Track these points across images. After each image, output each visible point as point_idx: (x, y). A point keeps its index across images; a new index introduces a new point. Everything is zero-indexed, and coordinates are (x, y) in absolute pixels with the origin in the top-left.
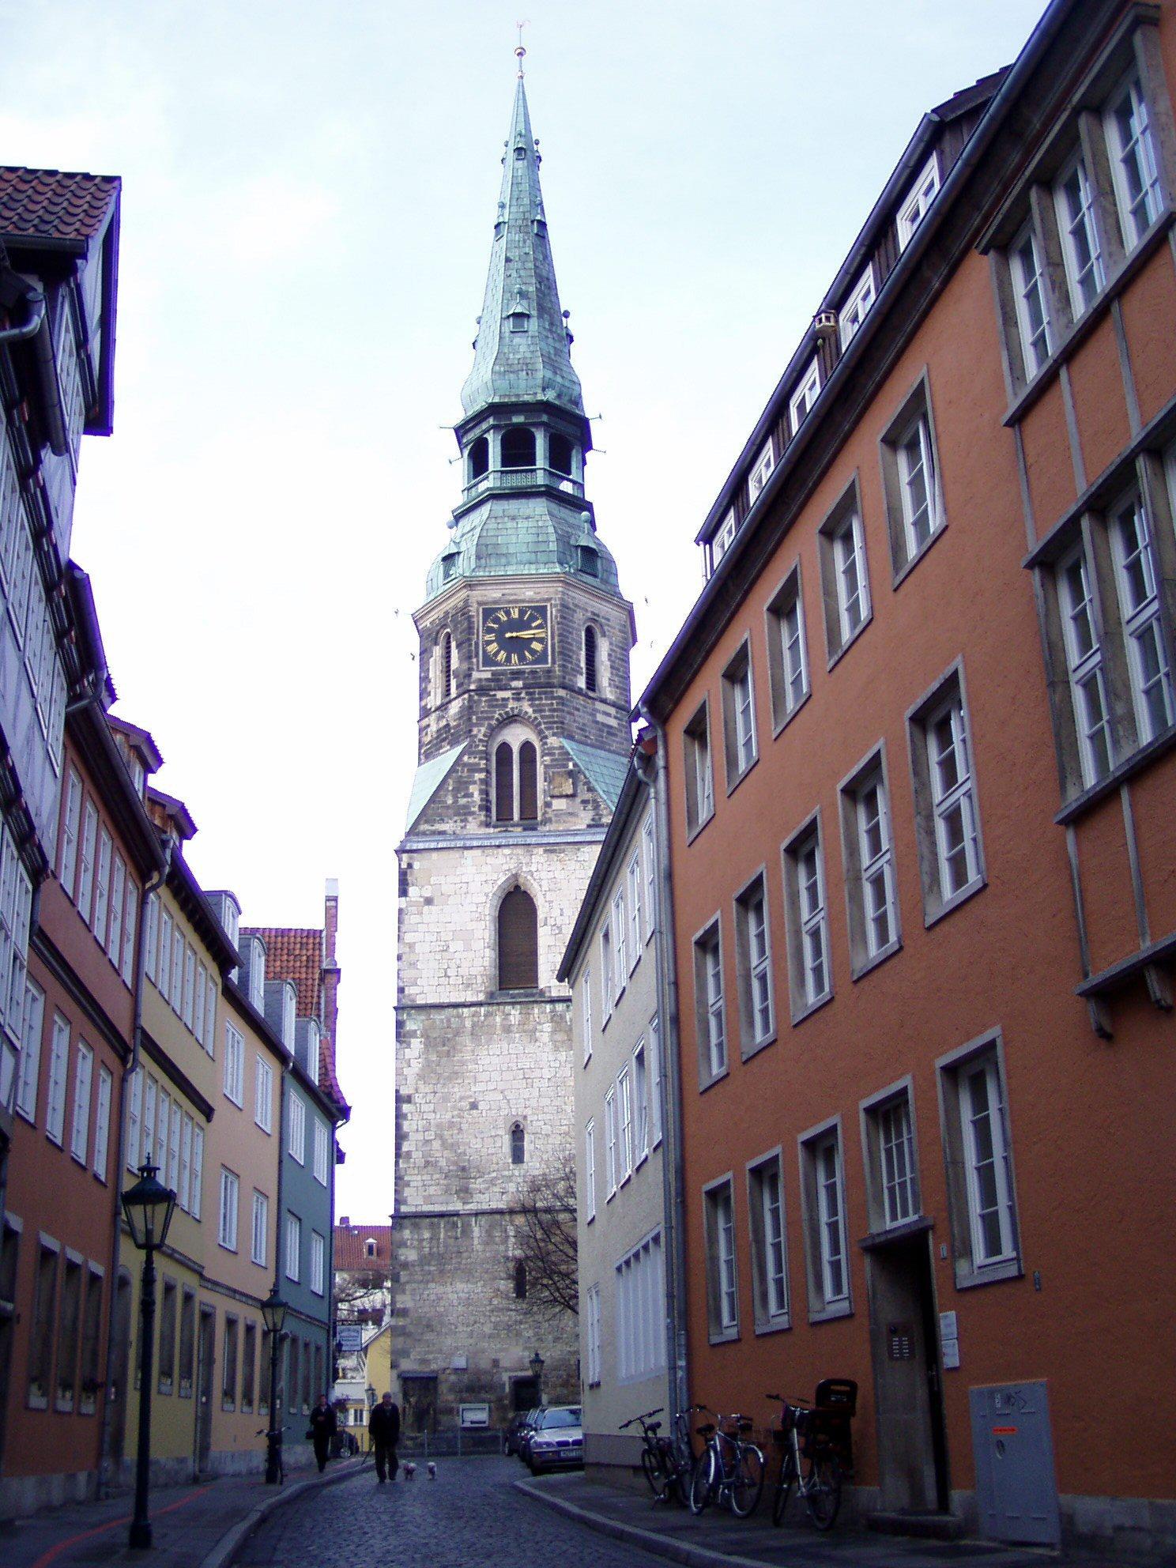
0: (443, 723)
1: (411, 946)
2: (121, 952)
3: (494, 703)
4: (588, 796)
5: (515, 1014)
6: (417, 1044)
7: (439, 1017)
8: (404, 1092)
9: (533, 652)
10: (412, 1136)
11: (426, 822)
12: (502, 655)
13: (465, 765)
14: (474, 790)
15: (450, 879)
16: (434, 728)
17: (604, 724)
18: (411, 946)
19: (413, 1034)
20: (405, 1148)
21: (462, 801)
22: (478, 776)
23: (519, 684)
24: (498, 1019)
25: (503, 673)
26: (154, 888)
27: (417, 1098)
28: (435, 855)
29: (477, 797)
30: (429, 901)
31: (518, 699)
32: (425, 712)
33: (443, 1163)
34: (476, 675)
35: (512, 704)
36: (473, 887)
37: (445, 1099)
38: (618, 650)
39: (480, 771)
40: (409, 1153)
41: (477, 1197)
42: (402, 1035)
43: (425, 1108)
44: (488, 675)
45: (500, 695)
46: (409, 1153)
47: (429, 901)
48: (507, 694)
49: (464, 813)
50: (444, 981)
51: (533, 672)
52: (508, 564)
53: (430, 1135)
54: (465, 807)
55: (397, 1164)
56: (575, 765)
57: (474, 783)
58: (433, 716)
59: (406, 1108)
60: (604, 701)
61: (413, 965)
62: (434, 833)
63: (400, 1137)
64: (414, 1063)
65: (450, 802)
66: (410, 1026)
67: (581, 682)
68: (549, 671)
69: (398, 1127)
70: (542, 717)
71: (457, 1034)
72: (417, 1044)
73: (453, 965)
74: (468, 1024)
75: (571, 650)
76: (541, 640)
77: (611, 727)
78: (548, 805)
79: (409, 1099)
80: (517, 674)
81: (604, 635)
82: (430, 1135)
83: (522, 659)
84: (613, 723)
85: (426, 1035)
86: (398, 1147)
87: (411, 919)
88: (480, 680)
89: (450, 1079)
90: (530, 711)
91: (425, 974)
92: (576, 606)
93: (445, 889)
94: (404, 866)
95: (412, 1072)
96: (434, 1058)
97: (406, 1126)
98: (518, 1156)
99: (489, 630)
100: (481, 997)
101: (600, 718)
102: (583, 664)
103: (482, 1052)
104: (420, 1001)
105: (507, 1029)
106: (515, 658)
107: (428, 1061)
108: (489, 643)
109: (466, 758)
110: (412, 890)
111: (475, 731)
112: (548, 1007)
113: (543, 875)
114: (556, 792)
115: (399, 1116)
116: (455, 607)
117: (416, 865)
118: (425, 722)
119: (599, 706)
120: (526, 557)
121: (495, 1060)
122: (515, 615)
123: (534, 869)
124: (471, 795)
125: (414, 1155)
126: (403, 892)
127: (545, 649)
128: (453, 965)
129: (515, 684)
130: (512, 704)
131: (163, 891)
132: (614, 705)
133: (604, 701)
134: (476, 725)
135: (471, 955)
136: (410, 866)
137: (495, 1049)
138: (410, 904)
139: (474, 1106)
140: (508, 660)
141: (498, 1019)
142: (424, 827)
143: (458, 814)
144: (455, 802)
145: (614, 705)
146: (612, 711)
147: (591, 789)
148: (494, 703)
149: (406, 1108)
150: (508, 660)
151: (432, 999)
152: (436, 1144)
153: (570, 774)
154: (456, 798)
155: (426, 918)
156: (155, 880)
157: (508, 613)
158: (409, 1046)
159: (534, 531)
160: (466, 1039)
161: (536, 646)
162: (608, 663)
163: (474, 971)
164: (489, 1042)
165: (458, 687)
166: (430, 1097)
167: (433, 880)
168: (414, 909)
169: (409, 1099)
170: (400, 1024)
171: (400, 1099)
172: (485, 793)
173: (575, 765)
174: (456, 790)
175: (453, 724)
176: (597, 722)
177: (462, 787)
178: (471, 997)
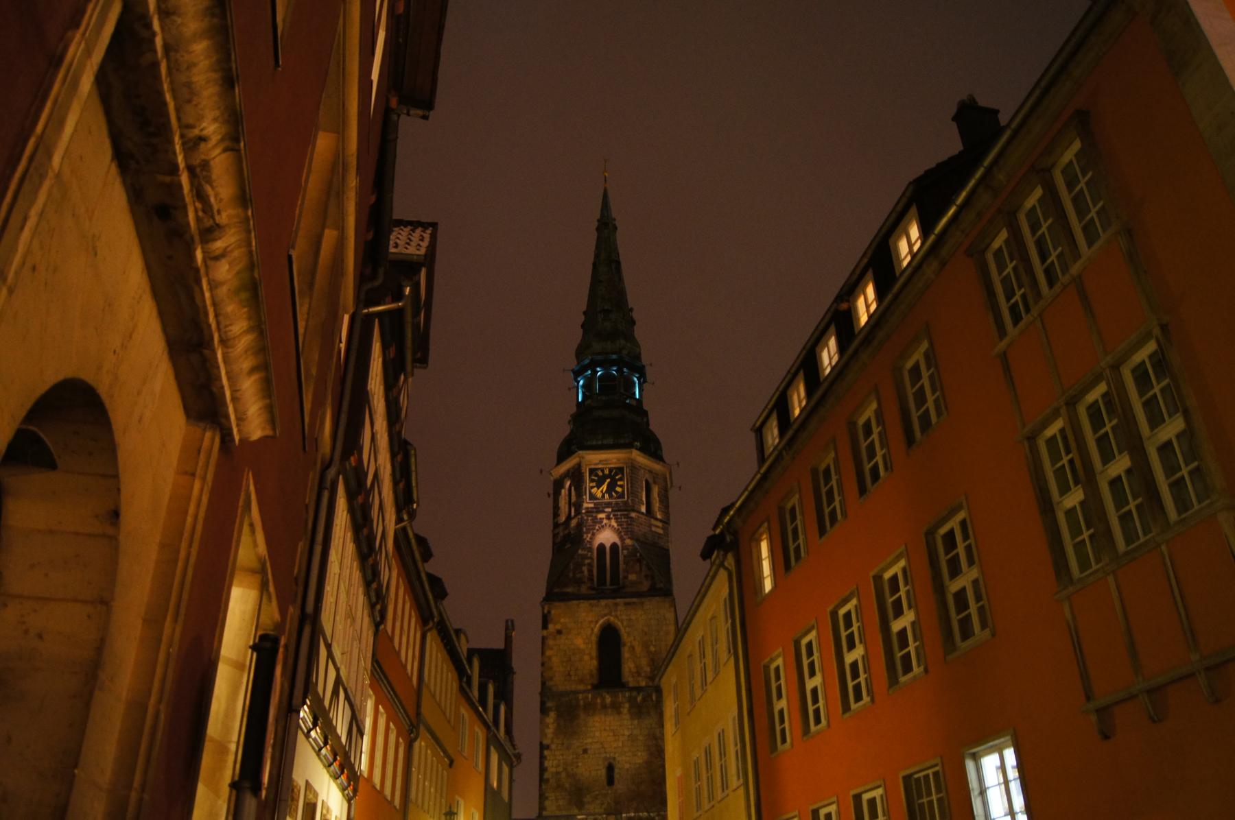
0: (566, 532)
1: (550, 658)
2: (412, 668)
6: (552, 715)
8: (546, 742)
9: (617, 492)
14: (585, 569)
16: (561, 534)
17: (656, 532)
20: (546, 776)
21: (578, 576)
22: (587, 561)
23: (610, 510)
24: (599, 701)
26: (430, 629)
27: (553, 747)
29: (586, 573)
30: (559, 632)
32: (556, 525)
33: (567, 786)
34: (585, 505)
39: (588, 558)
40: (548, 780)
41: (587, 806)
42: (544, 711)
44: (592, 505)
46: (548, 780)
47: (559, 632)
53: (560, 769)
55: (540, 786)
56: (641, 555)
57: (585, 565)
58: (561, 528)
59: (546, 753)
60: (656, 519)
63: (542, 770)
64: (551, 726)
66: (549, 704)
67: (643, 509)
69: (541, 764)
70: (622, 528)
72: (552, 715)
75: (638, 492)
76: (621, 486)
77: (659, 534)
78: (626, 578)
79: (548, 747)
80: (608, 505)
81: (655, 483)
83: (611, 496)
84: (661, 531)
86: (541, 775)
87: (550, 642)
88: (587, 508)
92: (640, 467)
94: (546, 611)
95: (550, 731)
97: (546, 764)
98: (610, 781)
99: (592, 481)
101: (654, 529)
102: (644, 499)
105: (604, 707)
108: (592, 487)
110: (551, 626)
111: (585, 536)
115: (542, 758)
116: (573, 467)
117: (553, 612)
118: (556, 531)
119: (653, 521)
121: (597, 724)
122: (607, 472)
125: (551, 781)
126: (545, 627)
127: (623, 491)
129: (607, 510)
131: (435, 632)
132: (661, 521)
133: (656, 519)
136: (549, 612)
137: (597, 718)
139: (585, 751)
141: (599, 701)
145: (661, 521)
146: (660, 524)
149: (546, 753)
152: (563, 775)
156: (431, 624)
157: (603, 471)
161: (618, 489)
165: (575, 512)
167: (562, 620)
169: (548, 747)
170: (543, 704)
171: (543, 747)
172: (590, 571)
175: (572, 532)
176: (653, 531)
178: (581, 687)
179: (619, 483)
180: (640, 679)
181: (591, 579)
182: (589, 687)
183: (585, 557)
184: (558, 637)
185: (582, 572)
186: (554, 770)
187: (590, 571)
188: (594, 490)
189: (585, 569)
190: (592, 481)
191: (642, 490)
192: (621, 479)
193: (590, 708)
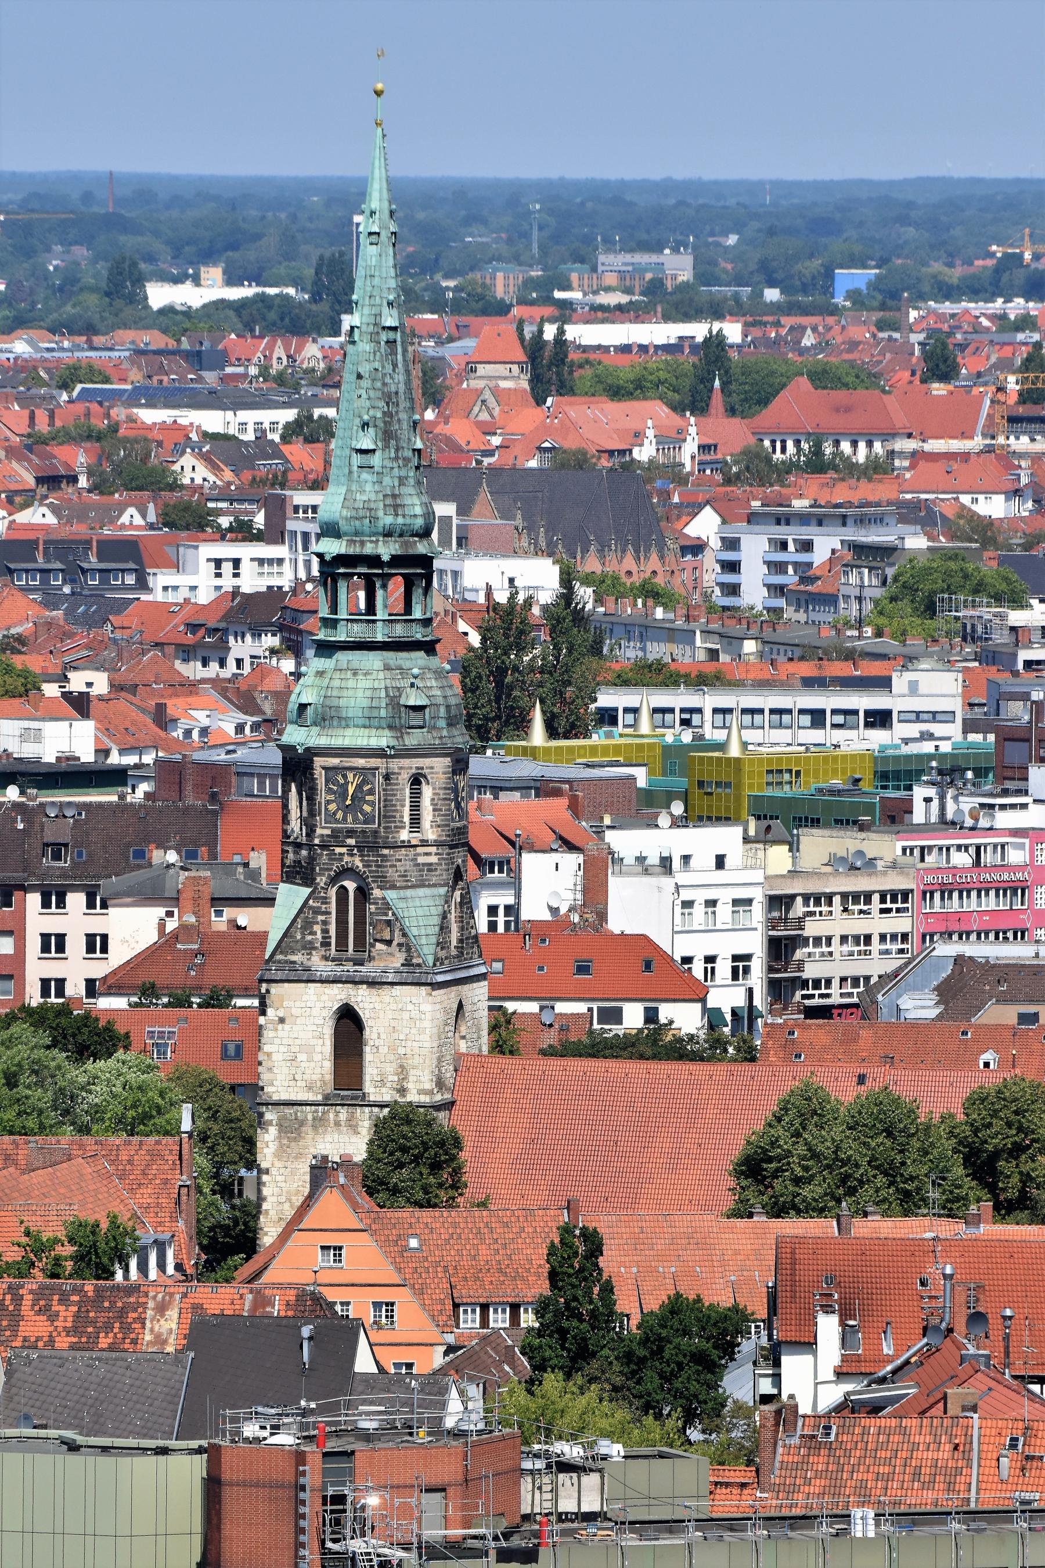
1: (269, 1055)
3: (333, 858)
4: (403, 940)
5: (343, 1113)
7: (289, 1111)
10: (269, 1199)
11: (281, 953)
12: (340, 815)
13: (311, 908)
14: (317, 928)
15: (298, 1004)
17: (424, 864)
18: (269, 1055)
19: (270, 1123)
21: (309, 938)
22: (320, 918)
23: (352, 841)
24: (331, 1116)
25: (340, 831)
28: (286, 985)
29: (319, 936)
30: (282, 1020)
31: (352, 855)
35: (346, 858)
36: (315, 1012)
37: (293, 1173)
38: (441, 792)
43: (279, 1178)
44: (328, 832)
45: (338, 850)
47: (282, 1020)
48: (344, 850)
49: (309, 947)
50: (292, 1083)
51: (363, 832)
52: (347, 726)
54: (311, 942)
56: (394, 914)
59: (265, 1178)
61: (270, 1070)
62: (286, 962)
64: (271, 1144)
65: (299, 937)
68: (376, 832)
71: (302, 1123)
73: (299, 1072)
74: (310, 1117)
76: (372, 804)
77: (431, 864)
80: (351, 833)
82: (283, 1199)
83: (355, 820)
85: (280, 1125)
87: (268, 1034)
89: (296, 1158)
90: (360, 865)
91: (279, 1077)
93: (294, 1011)
94: (263, 991)
96: (285, 1141)
100: (320, 1098)
103: (320, 1140)
104: (275, 1097)
105: (337, 1124)
106: (350, 818)
107: (281, 1146)
108: (328, 802)
109: (311, 902)
110: (270, 1011)
111: (318, 880)
112: (367, 1110)
113: (366, 1005)
114: (378, 937)
117: (273, 991)
120: (360, 722)
123: (359, 999)
124: (315, 933)
125: (271, 1213)
128: (299, 1072)
130: (346, 858)
134: (320, 875)
135: (312, 1064)
136: (268, 991)
137: (328, 1138)
138: (267, 1022)
140: (345, 819)
141: (331, 1116)
142: (279, 957)
143: (304, 948)
144: (303, 938)
147: (405, 935)
148: (333, 858)
149: (265, 1178)
150: (345, 819)
151: (284, 1096)
153: (389, 923)
154: (303, 934)
155: (280, 1034)
158: (267, 1131)
159: (369, 693)
160: (308, 1129)
161: (367, 808)
162: (431, 808)
163: (314, 1077)
164: (325, 1132)
166: (282, 1170)
168: (270, 1026)
169: (267, 1172)
172: (325, 931)
173: (394, 914)
174: (304, 928)
177: (308, 926)
178: (311, 1097)
179: (368, 798)
180: (384, 1090)
181: (326, 944)
182: (320, 1098)
183: (317, 912)
184: (280, 1026)
185: (314, 933)
186: (274, 1199)
187: (325, 931)
188: (332, 807)
189: (317, 928)
190: (329, 791)
191: (403, 806)
192: (371, 792)
193: (319, 1123)
